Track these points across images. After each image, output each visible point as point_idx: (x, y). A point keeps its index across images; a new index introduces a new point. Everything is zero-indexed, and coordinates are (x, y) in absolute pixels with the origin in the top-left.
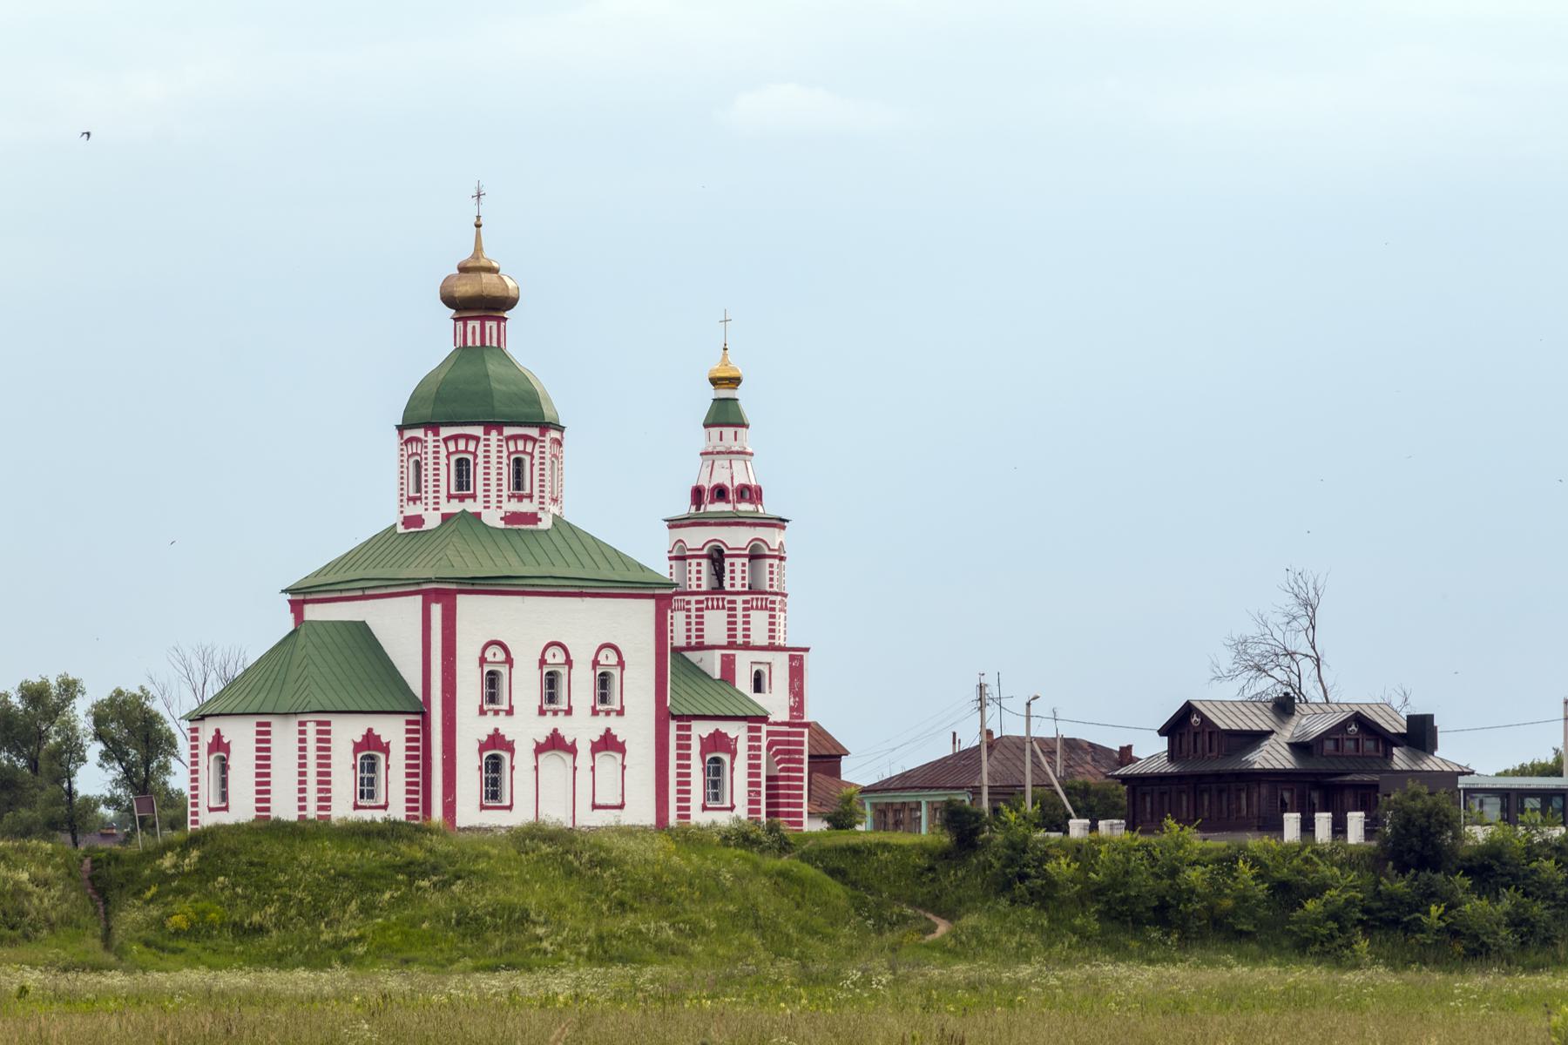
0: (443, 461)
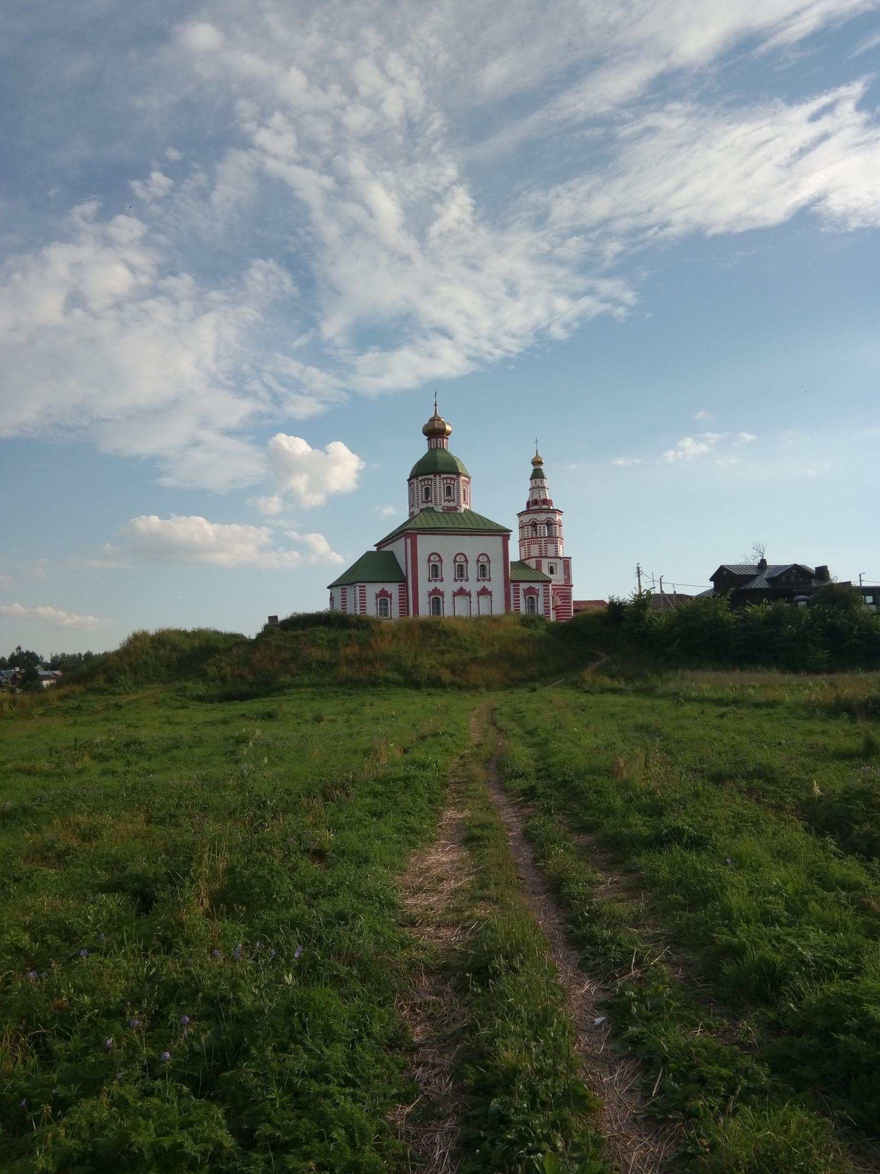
0: (420, 489)
